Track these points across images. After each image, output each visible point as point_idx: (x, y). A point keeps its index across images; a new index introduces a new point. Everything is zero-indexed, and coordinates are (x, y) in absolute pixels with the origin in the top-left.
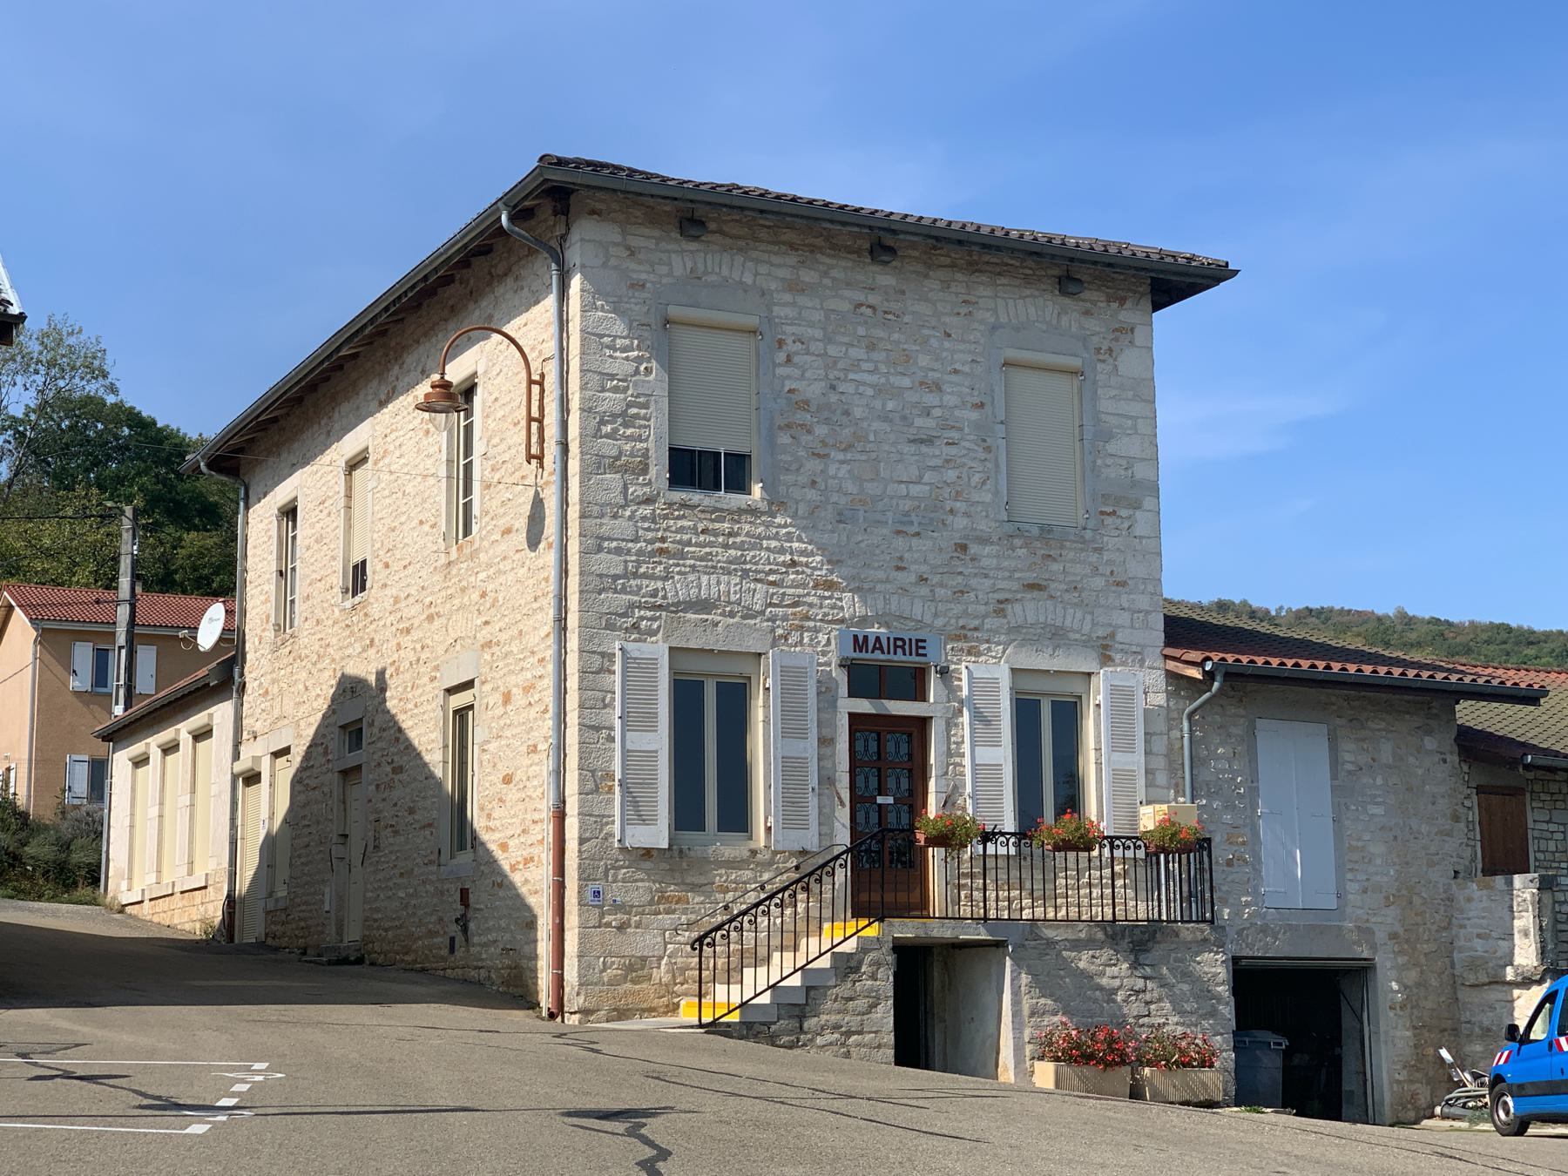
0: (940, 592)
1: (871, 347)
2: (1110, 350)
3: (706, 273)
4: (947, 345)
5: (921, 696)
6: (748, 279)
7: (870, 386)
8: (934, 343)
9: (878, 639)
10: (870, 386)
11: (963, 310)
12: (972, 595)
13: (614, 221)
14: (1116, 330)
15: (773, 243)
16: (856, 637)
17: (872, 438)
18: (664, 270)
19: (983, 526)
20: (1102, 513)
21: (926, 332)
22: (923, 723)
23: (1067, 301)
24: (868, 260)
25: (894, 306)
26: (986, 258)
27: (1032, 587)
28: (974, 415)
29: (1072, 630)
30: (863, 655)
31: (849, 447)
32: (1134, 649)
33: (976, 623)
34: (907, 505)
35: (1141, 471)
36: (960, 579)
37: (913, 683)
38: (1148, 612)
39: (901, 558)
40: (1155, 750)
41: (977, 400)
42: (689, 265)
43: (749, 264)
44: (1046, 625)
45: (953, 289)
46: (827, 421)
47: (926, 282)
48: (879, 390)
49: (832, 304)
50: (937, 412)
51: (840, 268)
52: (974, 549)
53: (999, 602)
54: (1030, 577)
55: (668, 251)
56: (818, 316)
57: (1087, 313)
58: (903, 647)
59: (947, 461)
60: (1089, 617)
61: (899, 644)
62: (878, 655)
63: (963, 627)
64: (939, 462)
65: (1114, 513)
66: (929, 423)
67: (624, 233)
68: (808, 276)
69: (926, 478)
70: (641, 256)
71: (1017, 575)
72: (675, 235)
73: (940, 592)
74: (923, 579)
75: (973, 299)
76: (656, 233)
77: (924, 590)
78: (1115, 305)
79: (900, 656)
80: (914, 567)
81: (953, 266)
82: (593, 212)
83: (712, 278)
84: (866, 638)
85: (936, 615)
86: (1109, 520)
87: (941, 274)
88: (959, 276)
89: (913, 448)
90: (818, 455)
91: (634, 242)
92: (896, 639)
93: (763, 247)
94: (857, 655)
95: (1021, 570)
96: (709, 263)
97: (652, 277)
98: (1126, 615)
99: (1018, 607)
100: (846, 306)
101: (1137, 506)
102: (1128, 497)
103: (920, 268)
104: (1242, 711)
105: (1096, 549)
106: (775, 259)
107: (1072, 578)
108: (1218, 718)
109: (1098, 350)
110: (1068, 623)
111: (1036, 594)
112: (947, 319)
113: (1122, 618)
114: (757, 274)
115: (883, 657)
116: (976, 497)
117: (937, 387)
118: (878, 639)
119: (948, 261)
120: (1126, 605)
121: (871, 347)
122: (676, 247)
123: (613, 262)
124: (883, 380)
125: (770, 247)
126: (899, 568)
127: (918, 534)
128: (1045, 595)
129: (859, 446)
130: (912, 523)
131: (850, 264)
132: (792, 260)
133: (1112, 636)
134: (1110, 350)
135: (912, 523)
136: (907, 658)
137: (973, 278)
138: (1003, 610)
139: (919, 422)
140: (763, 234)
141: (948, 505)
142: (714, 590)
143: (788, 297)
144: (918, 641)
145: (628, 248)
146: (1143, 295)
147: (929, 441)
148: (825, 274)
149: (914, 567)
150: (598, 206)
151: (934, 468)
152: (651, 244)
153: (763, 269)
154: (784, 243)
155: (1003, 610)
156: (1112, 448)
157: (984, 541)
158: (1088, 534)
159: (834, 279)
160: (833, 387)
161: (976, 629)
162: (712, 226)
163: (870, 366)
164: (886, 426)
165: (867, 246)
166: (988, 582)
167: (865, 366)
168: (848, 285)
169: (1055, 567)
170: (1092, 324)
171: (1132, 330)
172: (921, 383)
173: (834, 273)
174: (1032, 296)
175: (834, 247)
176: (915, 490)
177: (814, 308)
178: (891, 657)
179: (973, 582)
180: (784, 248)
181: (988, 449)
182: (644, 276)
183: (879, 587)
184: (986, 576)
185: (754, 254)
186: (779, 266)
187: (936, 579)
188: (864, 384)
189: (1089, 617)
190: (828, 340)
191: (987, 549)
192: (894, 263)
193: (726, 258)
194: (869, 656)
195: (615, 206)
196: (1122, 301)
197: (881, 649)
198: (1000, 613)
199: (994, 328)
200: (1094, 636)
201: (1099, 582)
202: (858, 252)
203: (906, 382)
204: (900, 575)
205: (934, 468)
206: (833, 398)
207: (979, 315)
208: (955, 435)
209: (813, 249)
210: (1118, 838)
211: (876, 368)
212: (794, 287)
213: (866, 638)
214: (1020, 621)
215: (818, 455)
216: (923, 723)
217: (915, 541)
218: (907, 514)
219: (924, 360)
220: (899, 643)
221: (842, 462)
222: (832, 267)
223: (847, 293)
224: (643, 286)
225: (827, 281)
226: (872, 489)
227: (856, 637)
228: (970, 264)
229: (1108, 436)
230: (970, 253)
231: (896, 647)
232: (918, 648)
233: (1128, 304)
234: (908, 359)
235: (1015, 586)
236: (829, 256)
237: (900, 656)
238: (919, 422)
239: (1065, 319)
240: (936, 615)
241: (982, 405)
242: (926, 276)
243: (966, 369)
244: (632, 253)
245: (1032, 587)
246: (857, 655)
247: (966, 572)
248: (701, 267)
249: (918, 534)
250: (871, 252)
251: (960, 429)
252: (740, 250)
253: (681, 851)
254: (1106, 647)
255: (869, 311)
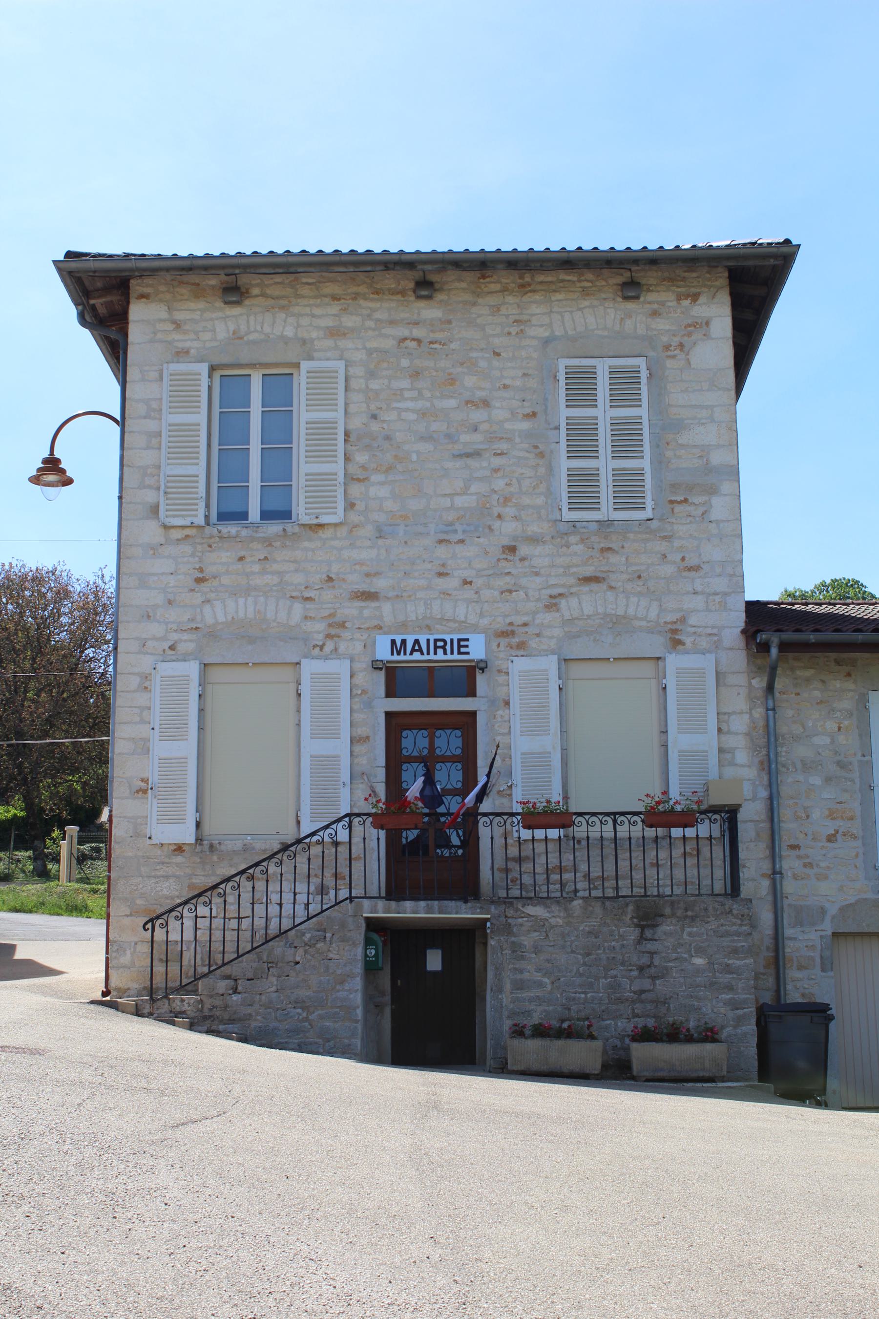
0: (486, 594)
1: (416, 374)
2: (681, 346)
3: (247, 334)
4: (496, 363)
5: (471, 692)
6: (289, 332)
7: (413, 411)
8: (483, 364)
9: (417, 642)
10: (413, 411)
11: (514, 330)
12: (521, 593)
13: (161, 301)
14: (689, 325)
15: (316, 297)
16: (393, 642)
17: (414, 457)
18: (207, 336)
19: (534, 528)
20: (671, 502)
21: (474, 354)
22: (473, 714)
23: (630, 305)
24: (413, 298)
25: (439, 336)
26: (540, 278)
27: (588, 580)
28: (525, 425)
29: (636, 618)
30: (402, 657)
31: (390, 469)
32: (709, 631)
33: (525, 619)
34: (450, 517)
35: (717, 458)
36: (508, 579)
37: (465, 678)
38: (725, 594)
39: (443, 565)
40: (733, 728)
41: (528, 411)
42: (232, 327)
43: (291, 320)
44: (606, 615)
45: (504, 311)
46: (368, 447)
47: (474, 310)
48: (423, 414)
49: (372, 344)
50: (484, 427)
51: (384, 309)
52: (524, 550)
53: (551, 596)
54: (589, 571)
55: (212, 319)
56: (360, 356)
57: (655, 314)
58: (444, 647)
59: (496, 470)
60: (655, 604)
61: (440, 645)
62: (417, 656)
63: (511, 624)
64: (488, 473)
65: (686, 501)
66: (478, 437)
67: (170, 309)
68: (349, 321)
69: (473, 489)
70: (187, 327)
71: (575, 570)
72: (219, 304)
73: (486, 594)
74: (466, 582)
75: (525, 318)
76: (201, 305)
77: (468, 593)
78: (686, 303)
79: (440, 655)
80: (456, 573)
81: (504, 290)
82: (142, 296)
83: (253, 337)
84: (404, 642)
85: (482, 615)
86: (678, 508)
87: (492, 300)
88: (510, 299)
89: (459, 463)
90: (359, 480)
91: (179, 316)
92: (436, 641)
93: (305, 302)
94: (396, 657)
95: (577, 566)
96: (252, 323)
97: (196, 344)
98: (700, 598)
99: (574, 602)
100: (389, 344)
101: (713, 490)
102: (706, 486)
103: (468, 297)
104: (850, 685)
105: (665, 538)
106: (318, 311)
107: (634, 568)
108: (817, 694)
109: (667, 348)
110: (631, 611)
111: (594, 586)
112: (497, 341)
113: (698, 602)
114: (298, 326)
115: (425, 657)
116: (526, 501)
117: (486, 403)
118: (417, 642)
119: (498, 287)
120: (699, 588)
121: (416, 374)
122: (220, 314)
123: (159, 336)
124: (428, 404)
125: (312, 302)
126: (440, 574)
127: (462, 541)
128: (604, 586)
129: (400, 468)
130: (456, 531)
131: (393, 305)
132: (334, 309)
133: (683, 620)
134: (681, 346)
135: (456, 531)
136: (449, 657)
137: (526, 298)
138: (555, 605)
139: (464, 438)
140: (305, 291)
141: (496, 510)
142: (251, 609)
143: (329, 343)
144: (459, 640)
145: (174, 322)
146: (719, 288)
147: (477, 454)
148: (369, 316)
149: (456, 573)
150: (146, 290)
151: (481, 479)
152: (196, 316)
153: (305, 321)
154: (325, 296)
155: (555, 605)
156: (684, 438)
157: (534, 540)
158: (654, 524)
159: (378, 320)
160: (374, 417)
161: (525, 625)
162: (256, 291)
163: (415, 394)
164: (429, 447)
165: (412, 285)
166: (538, 580)
167: (407, 394)
168: (392, 323)
169: (613, 559)
170: (661, 324)
171: (707, 324)
172: (467, 402)
173: (377, 315)
174: (593, 307)
175: (377, 293)
176: (459, 501)
177: (357, 349)
178: (432, 657)
179: (524, 581)
180: (326, 300)
181: (541, 455)
182: (188, 344)
183: (420, 595)
184: (537, 574)
185: (296, 309)
186: (320, 317)
187: (479, 582)
188: (407, 410)
189: (655, 604)
190: (371, 375)
191: (539, 549)
192: (440, 296)
193: (268, 316)
194: (408, 657)
195: (162, 288)
196: (695, 297)
197: (420, 650)
198: (552, 605)
199: (546, 342)
200: (662, 621)
201: (668, 570)
202: (403, 293)
203: (452, 403)
204: (440, 581)
205: (481, 479)
206: (375, 427)
207: (531, 332)
208: (504, 446)
209: (356, 297)
210: (622, 814)
211: (420, 393)
212: (335, 333)
213: (404, 642)
214: (576, 614)
215: (359, 480)
216: (473, 714)
217: (459, 548)
218: (451, 524)
219: (470, 381)
220: (440, 644)
221: (382, 484)
222: (373, 310)
223: (389, 331)
224: (187, 352)
225: (370, 324)
226: (415, 505)
227: (393, 642)
228: (522, 286)
229: (679, 426)
230: (521, 277)
231: (436, 647)
232: (459, 646)
233: (702, 299)
234: (452, 380)
235: (572, 581)
236: (372, 300)
237: (440, 655)
238: (464, 438)
239: (629, 323)
240: (482, 615)
241: (534, 414)
242: (474, 304)
243: (518, 383)
244: (178, 325)
245: (588, 580)
246: (396, 657)
247: (514, 571)
248: (243, 328)
249: (462, 541)
250: (414, 292)
251: (509, 440)
252: (282, 308)
253: (211, 846)
254: (675, 631)
255: (413, 344)
